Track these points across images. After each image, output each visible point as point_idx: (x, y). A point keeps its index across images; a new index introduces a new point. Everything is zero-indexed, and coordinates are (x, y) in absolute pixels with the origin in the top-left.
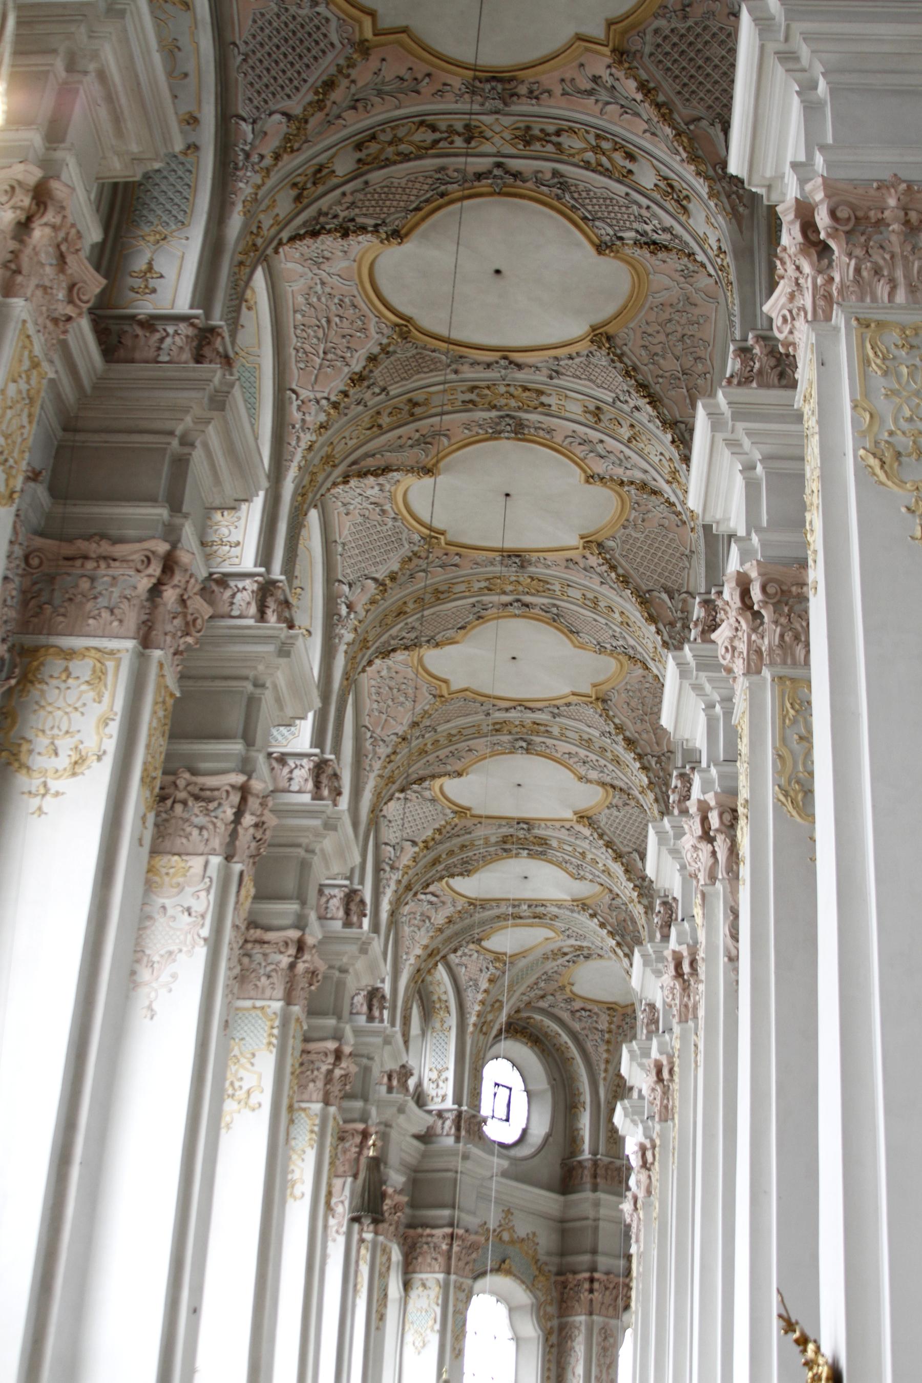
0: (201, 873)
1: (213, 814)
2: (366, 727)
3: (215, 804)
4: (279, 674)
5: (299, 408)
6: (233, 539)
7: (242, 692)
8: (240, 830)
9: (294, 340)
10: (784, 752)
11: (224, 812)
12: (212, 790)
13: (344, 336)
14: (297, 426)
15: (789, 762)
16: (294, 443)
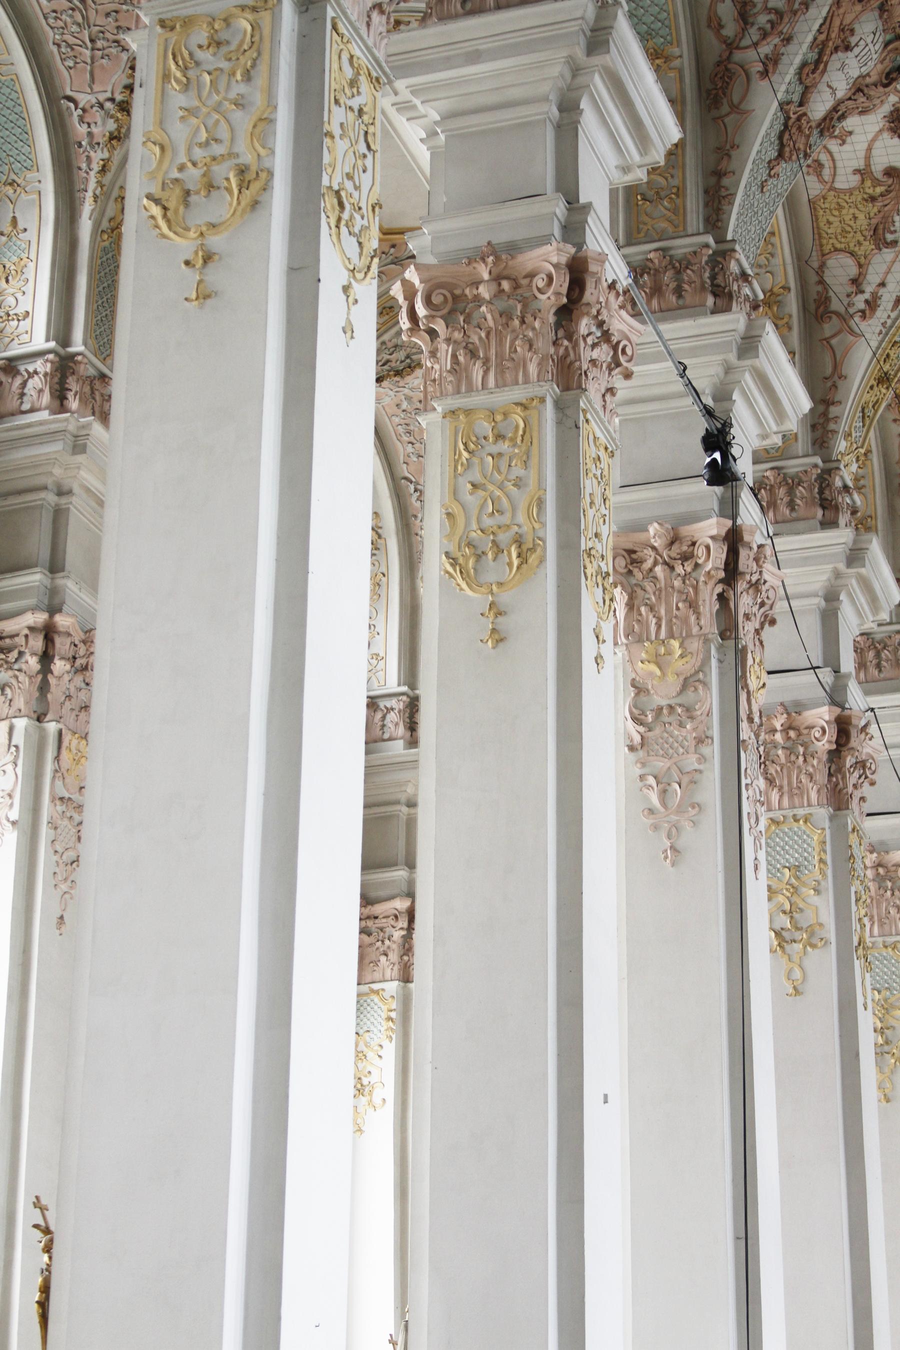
0: (7, 742)
1: (16, 667)
2: (406, 478)
3: (15, 654)
4: (83, 473)
5: (81, 119)
6: (20, 310)
7: (42, 506)
8: (52, 680)
9: (50, 33)
10: (456, 509)
11: (27, 662)
12: (12, 637)
13: (108, 15)
14: (84, 143)
15: (461, 521)
16: (84, 166)
